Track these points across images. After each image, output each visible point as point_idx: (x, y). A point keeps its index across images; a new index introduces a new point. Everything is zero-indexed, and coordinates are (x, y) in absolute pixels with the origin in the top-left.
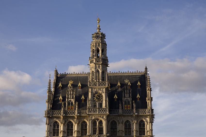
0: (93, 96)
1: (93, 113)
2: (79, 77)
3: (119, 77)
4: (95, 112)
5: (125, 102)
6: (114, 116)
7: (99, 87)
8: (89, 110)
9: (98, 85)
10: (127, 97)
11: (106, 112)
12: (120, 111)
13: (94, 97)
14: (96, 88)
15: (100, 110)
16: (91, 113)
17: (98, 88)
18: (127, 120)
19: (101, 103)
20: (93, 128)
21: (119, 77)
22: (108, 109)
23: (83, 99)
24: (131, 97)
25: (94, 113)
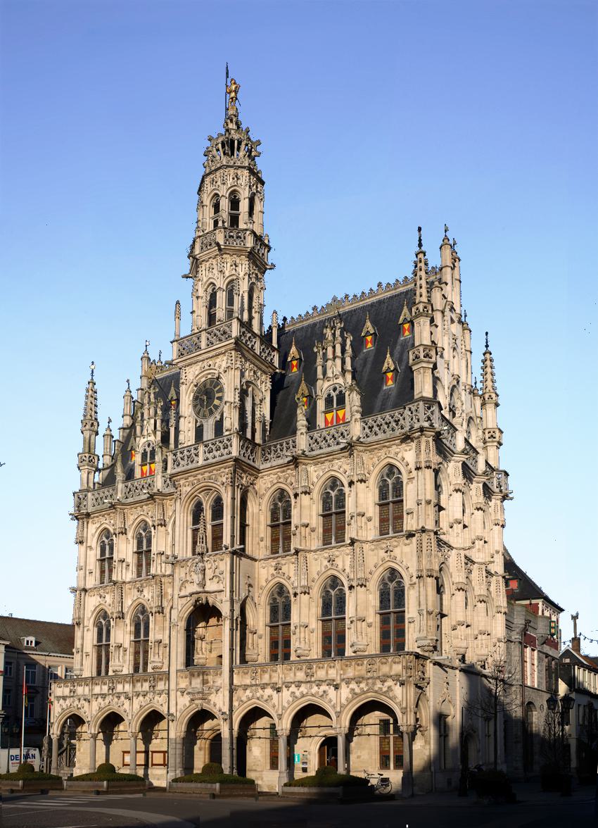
0: (191, 398)
9: (203, 345)
10: (334, 374)
12: (302, 441)
14: (200, 358)
24: (349, 371)
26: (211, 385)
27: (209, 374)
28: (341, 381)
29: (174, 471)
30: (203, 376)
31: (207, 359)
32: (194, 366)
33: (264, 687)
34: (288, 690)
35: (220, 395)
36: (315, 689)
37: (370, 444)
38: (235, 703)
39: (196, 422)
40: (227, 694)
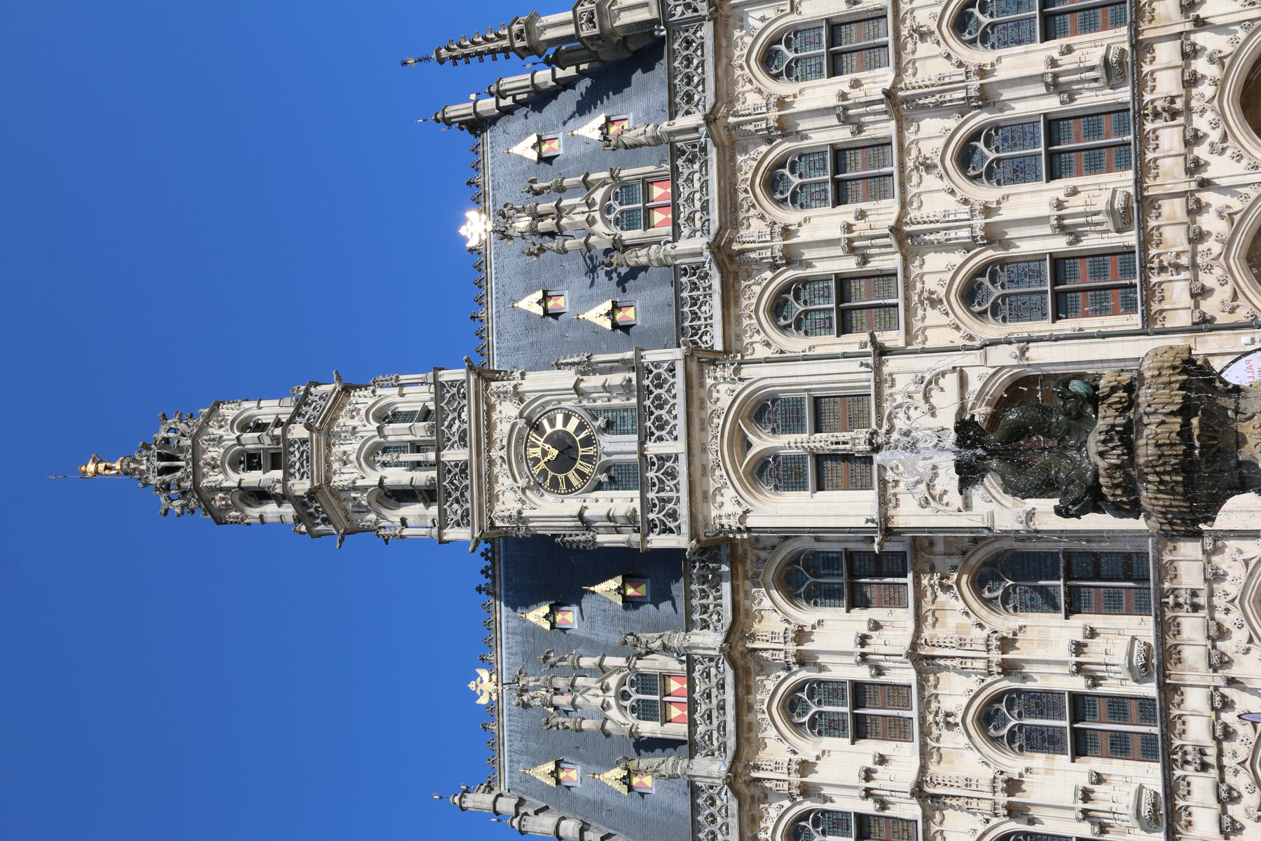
3: (502, 308)
4: (672, 475)
5: (627, 220)
8: (664, 531)
11: (671, 370)
16: (683, 510)
18: (758, 190)
19: (601, 422)
20: (820, 487)
21: (502, 308)
22: (650, 356)
25: (683, 479)
28: (598, 195)
29: (685, 529)
30: (518, 463)
31: (489, 451)
32: (498, 488)
33: (1198, 237)
34: (1207, 164)
35: (560, 418)
36: (1206, 90)
38: (1241, 315)
39: (599, 486)
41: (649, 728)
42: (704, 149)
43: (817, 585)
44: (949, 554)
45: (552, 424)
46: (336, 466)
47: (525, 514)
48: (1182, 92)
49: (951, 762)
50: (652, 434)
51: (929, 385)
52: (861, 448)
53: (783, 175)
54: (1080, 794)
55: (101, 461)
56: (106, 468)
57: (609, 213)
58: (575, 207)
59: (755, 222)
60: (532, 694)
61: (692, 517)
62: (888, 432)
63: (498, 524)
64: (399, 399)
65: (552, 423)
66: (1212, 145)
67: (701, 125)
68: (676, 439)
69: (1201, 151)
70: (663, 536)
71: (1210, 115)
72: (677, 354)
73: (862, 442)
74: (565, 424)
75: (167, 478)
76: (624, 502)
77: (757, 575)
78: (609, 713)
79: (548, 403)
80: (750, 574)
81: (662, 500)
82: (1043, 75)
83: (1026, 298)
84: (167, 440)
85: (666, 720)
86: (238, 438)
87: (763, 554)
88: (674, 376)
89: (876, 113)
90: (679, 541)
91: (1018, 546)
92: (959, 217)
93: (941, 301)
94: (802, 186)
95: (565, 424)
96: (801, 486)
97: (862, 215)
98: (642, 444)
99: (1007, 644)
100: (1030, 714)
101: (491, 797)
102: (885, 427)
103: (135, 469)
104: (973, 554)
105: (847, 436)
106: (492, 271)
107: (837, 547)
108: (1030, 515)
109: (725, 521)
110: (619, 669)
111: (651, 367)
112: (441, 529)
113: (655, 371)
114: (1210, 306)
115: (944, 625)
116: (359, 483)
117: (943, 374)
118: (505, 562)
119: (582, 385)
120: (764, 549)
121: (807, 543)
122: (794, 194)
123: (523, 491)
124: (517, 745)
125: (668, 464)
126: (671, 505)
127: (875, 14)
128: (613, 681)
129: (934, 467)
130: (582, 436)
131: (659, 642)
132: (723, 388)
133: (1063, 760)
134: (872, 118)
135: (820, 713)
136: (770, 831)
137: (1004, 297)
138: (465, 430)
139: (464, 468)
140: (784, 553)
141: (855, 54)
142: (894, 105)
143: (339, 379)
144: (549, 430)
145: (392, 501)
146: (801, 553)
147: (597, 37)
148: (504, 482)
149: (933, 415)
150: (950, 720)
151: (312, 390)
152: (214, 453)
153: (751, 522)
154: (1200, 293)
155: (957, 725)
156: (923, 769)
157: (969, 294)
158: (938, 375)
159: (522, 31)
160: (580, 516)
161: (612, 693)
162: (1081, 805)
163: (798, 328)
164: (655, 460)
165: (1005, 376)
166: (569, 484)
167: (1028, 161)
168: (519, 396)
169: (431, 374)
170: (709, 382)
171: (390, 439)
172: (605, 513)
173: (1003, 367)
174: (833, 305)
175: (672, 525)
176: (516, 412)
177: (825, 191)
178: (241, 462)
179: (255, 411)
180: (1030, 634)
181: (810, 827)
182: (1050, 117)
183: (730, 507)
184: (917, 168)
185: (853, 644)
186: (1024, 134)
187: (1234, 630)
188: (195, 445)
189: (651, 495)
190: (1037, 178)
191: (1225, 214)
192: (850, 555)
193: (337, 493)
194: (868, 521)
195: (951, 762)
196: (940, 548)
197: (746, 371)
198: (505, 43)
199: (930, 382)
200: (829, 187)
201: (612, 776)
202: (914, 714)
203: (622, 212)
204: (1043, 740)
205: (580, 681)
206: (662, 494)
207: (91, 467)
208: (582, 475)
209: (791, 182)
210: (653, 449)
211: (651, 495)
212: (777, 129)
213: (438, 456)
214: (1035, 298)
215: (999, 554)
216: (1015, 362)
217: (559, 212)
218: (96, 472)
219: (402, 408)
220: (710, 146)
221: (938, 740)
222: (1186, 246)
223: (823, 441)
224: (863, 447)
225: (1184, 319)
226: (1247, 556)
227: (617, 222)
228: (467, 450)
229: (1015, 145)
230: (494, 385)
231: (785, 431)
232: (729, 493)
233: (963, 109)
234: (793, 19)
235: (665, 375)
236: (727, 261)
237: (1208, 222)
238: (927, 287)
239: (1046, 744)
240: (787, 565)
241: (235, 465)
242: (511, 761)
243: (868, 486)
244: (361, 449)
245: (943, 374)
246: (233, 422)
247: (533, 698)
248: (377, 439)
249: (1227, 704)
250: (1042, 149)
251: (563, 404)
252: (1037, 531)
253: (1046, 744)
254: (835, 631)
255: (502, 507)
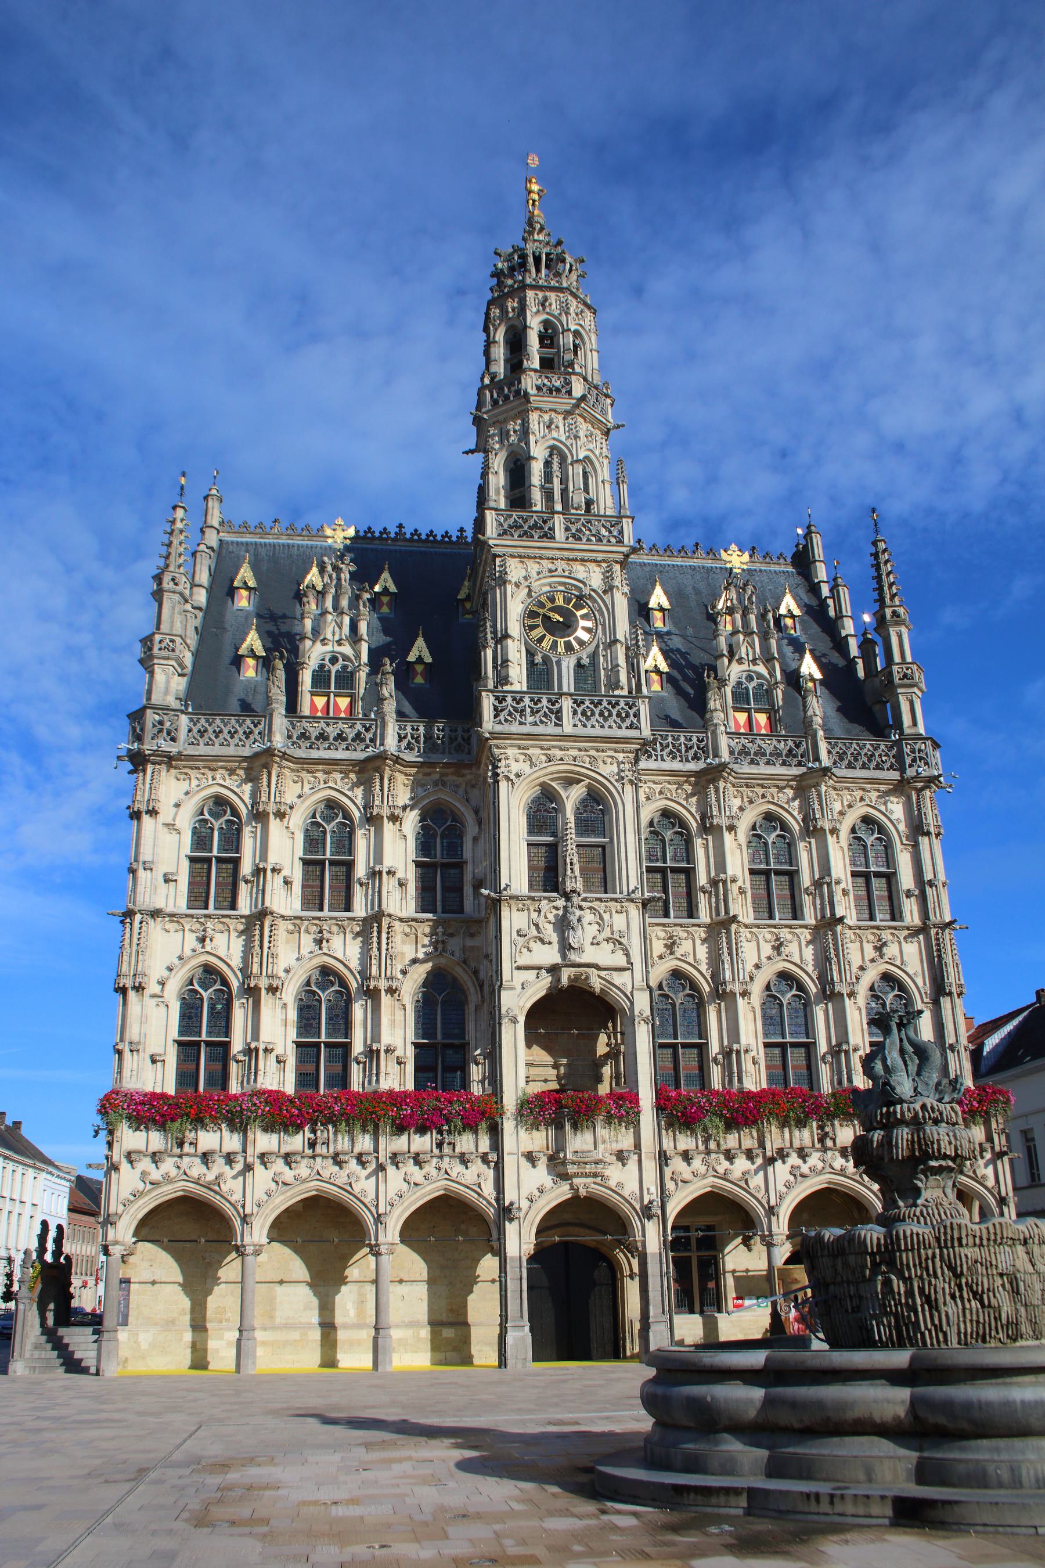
1: (527, 729)
2: (376, 550)
3: (647, 569)
6: (673, 773)
7: (566, 554)
8: (496, 709)
9: (559, 533)
11: (631, 727)
13: (529, 622)
15: (584, 713)
16: (515, 728)
17: (558, 554)
19: (586, 661)
21: (647, 569)
23: (420, 660)
26: (567, 601)
27: (564, 584)
28: (761, 669)
29: (499, 728)
31: (562, 559)
35: (589, 624)
37: (842, 779)
38: (670, 1185)
39: (530, 654)
40: (650, 1167)
41: (306, 678)
42: (799, 764)
43: (434, 836)
44: (464, 949)
45: (583, 617)
46: (546, 417)
47: (509, 587)
48: (839, 1144)
49: (288, 942)
50: (578, 706)
51: (616, 941)
52: (568, 883)
53: (775, 829)
54: (270, 1047)
55: (540, 197)
56: (534, 201)
57: (746, 678)
58: (753, 649)
59: (737, 802)
60: (334, 576)
61: (508, 736)
62: (581, 908)
63: (498, 560)
64: (600, 479)
65: (584, 617)
66: (799, 1167)
67: (820, 762)
68: (575, 725)
69: (794, 1159)
70: (492, 708)
71: (820, 1165)
72: (646, 732)
73: (573, 885)
74: (585, 629)
75: (531, 260)
76: (518, 676)
77: (444, 784)
78: (318, 644)
79: (602, 614)
80: (444, 778)
81: (523, 711)
82: (847, 1042)
83: (671, 1022)
84: (563, 261)
85: (313, 694)
86: (569, 330)
87: (461, 791)
88: (627, 728)
89: (823, 909)
90: (488, 723)
91: (471, 1007)
92: (741, 971)
93: (672, 953)
94: (766, 844)
95: (585, 629)
96: (530, 832)
97: (742, 891)
98: (571, 695)
99: (391, 991)
100: (329, 1009)
101: (216, 525)
102: (584, 904)
103: (534, 229)
104: (464, 969)
105: (577, 873)
106: (679, 561)
107: (468, 854)
108: (514, 1021)
109: (503, 762)
110: (358, 656)
111: (635, 709)
112: (496, 510)
113: (631, 712)
114: (677, 1164)
115: (404, 942)
116: (532, 438)
117: (628, 955)
118: (425, 552)
119: (619, 645)
120: (466, 792)
121: (471, 829)
122: (759, 836)
123: (529, 587)
124: (263, 552)
125: (553, 716)
126: (518, 717)
127: (896, 911)
128: (347, 649)
129: (550, 943)
130: (574, 643)
131: (387, 695)
132: (614, 768)
133: (292, 1034)
134: (818, 902)
135: (325, 832)
136: (221, 782)
137: (673, 1005)
138: (580, 539)
139: (549, 535)
140: (462, 809)
141: (865, 893)
142: (830, 924)
143: (618, 427)
144: (579, 613)
145: (512, 465)
146: (462, 824)
147: (891, 680)
148: (533, 567)
149: (592, 944)
150: (324, 942)
151: (609, 401)
152: (555, 308)
153: (503, 786)
154: (686, 1156)
155: (320, 948)
156: (283, 917)
157: (677, 974)
158: (627, 950)
159: (898, 616)
160: (506, 636)
161: (337, 649)
162: (262, 1047)
163: (651, 832)
164: (557, 706)
165: (626, 1004)
166: (532, 628)
167: (779, 1028)
168: (609, 589)
169: (628, 513)
170: (621, 756)
171: (570, 467)
172: (510, 657)
173: (632, 1003)
174: (669, 864)
175: (502, 717)
176: (595, 587)
177: (761, 863)
178: (546, 330)
179: (588, 347)
180: (399, 1013)
181: (226, 818)
182: (812, 1047)
183: (515, 767)
184: (778, 939)
185: (389, 864)
186: (800, 1026)
187: (424, 1171)
188: (560, 289)
189: (527, 700)
190: (766, 1035)
191: (747, 1176)
192: (460, 866)
193: (523, 415)
194: (507, 886)
195: (288, 942)
196: (469, 943)
197: (628, 788)
198: (887, 600)
199: (620, 943)
200: (763, 866)
201: (253, 641)
202: (326, 913)
203: (747, 689)
204: (308, 1019)
205: (347, 620)
206: (528, 710)
207: (535, 188)
208: (540, 640)
209: (769, 834)
210: (567, 705)
211: (527, 700)
212: (815, 827)
213: (558, 513)
214: (671, 1029)
215: (463, 992)
216: (636, 1013)
217: (748, 633)
218: (530, 192)
219: (591, 481)
220: (803, 770)
221: (307, 931)
222: (723, 1147)
223: (571, 852)
224: (569, 886)
225: (668, 1144)
226: (482, 1185)
227: (739, 683)
228: (563, 539)
229: (791, 1018)
230: (617, 567)
231: (577, 819)
232: (526, 768)
233: (824, 979)
234: (898, 846)
235: (628, 722)
236: (709, 777)
237: (742, 1164)
238: (684, 942)
239: (304, 1021)
240: (452, 811)
241: (546, 323)
242: (247, 544)
243: (531, 887)
244: (561, 442)
245: (628, 955)
246: (581, 325)
247: (330, 576)
248: (570, 460)
249: (362, 1164)
250: (788, 1039)
251: (600, 627)
252: (500, 1024)
253: (304, 1021)
254: (399, 848)
255: (513, 567)
